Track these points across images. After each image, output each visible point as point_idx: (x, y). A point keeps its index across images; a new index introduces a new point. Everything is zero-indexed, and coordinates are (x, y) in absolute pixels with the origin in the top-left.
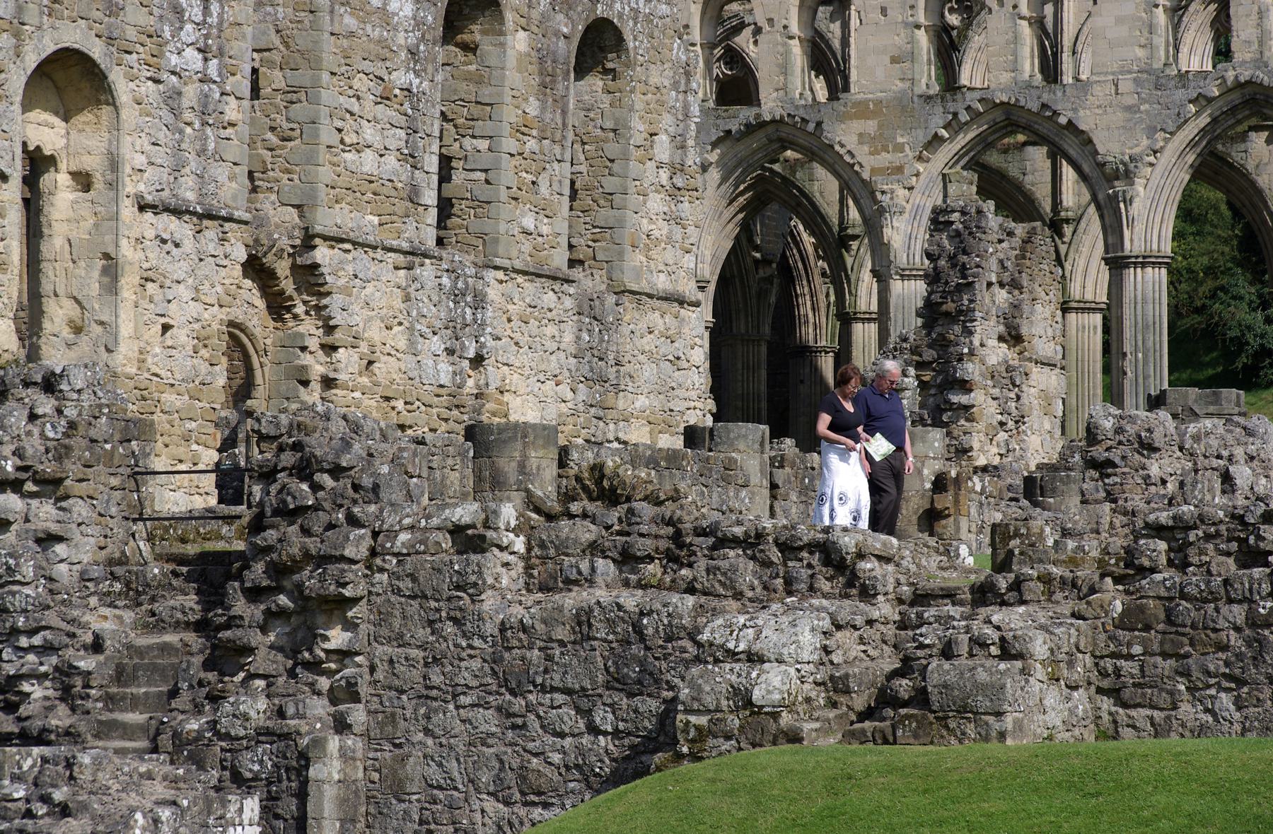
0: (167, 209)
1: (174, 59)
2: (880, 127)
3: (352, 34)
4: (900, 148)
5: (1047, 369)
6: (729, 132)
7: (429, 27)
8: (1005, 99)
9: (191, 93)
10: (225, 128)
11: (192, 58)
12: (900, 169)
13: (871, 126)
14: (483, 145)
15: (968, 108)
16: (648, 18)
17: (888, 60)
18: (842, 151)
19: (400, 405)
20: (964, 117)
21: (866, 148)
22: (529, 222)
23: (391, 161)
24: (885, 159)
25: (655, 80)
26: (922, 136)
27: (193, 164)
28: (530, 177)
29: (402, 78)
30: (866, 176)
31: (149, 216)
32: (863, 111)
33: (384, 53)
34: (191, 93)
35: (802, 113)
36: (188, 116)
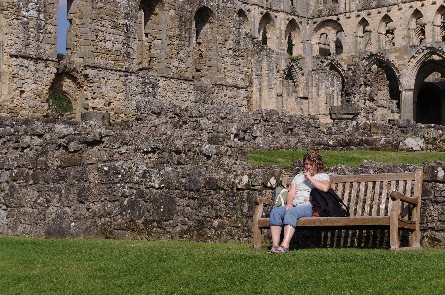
0: (21, 57)
1: (25, 13)
2: (400, 54)
3: (101, 8)
4: (404, 59)
5: (384, 108)
6: (365, 57)
7: (134, 7)
8: (430, 46)
9: (32, 24)
10: (48, 34)
11: (33, 13)
12: (405, 65)
13: (398, 54)
14: (159, 42)
15: (421, 49)
16: (223, 8)
17: (402, 38)
18: (391, 61)
19: (123, 115)
20: (420, 51)
21: (397, 60)
22: (176, 64)
23: (118, 46)
24: (401, 62)
25: (227, 25)
26: (410, 56)
27: (34, 44)
28: (175, 51)
29: (122, 21)
30: (396, 66)
31: (14, 59)
32: (396, 51)
33: (116, 14)
34: (32, 24)
35: (381, 52)
36: (32, 30)
